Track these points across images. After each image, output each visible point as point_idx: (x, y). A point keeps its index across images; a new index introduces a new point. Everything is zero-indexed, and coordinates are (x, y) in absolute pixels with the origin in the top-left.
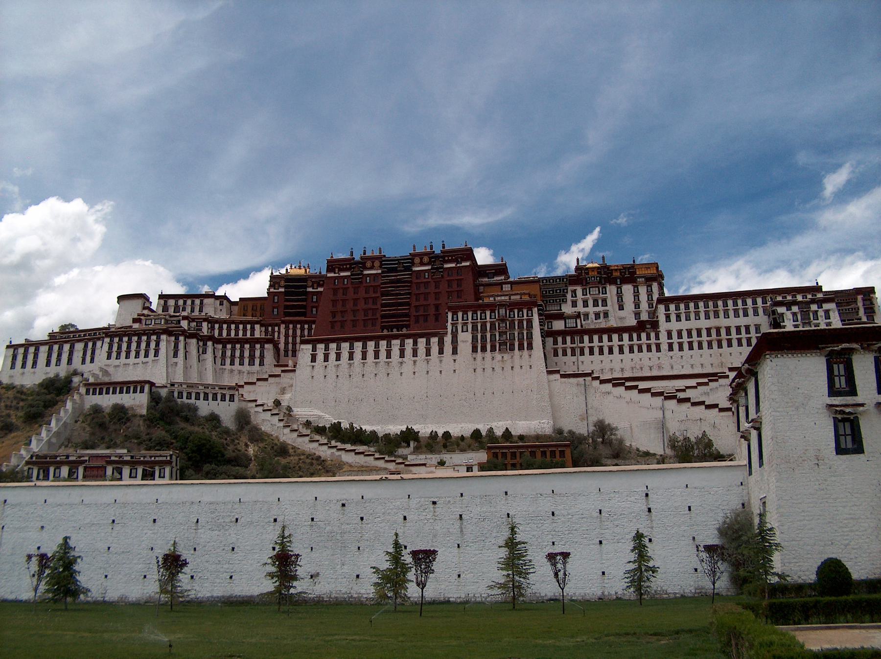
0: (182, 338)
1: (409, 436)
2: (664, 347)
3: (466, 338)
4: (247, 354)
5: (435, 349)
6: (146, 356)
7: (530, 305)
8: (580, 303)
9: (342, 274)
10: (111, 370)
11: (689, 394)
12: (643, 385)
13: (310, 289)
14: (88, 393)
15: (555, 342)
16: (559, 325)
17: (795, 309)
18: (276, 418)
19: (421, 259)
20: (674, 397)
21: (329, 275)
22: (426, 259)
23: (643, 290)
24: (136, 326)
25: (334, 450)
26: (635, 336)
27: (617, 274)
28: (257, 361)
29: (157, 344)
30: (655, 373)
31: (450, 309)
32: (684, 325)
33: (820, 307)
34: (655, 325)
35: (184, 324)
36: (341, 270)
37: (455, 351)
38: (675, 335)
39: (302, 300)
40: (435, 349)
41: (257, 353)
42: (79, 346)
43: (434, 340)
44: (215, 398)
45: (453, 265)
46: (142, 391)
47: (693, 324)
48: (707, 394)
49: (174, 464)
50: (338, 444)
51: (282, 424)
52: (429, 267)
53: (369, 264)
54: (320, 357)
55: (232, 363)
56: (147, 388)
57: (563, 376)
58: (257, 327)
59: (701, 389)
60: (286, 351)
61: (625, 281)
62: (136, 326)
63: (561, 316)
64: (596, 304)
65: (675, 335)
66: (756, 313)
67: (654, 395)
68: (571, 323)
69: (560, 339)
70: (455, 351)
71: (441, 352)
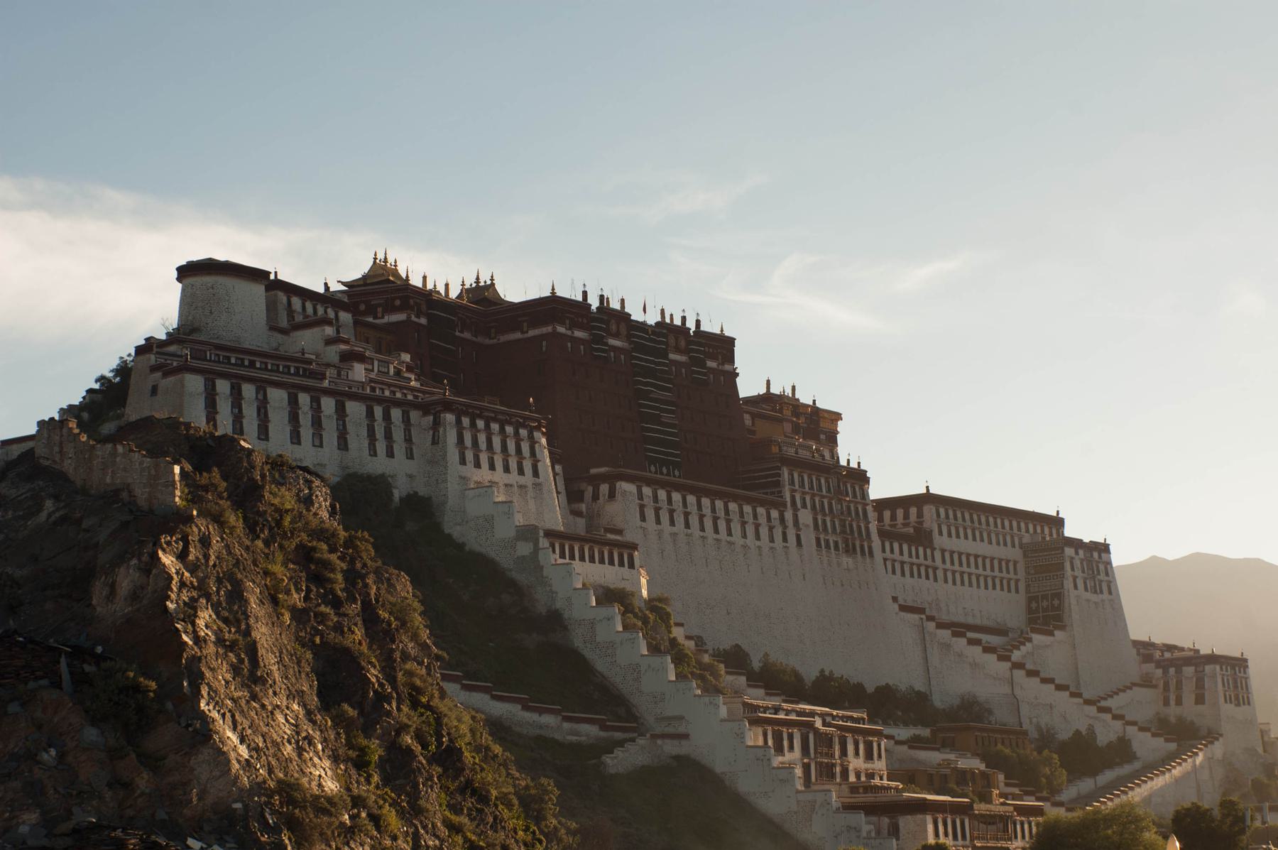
3: (806, 517)
6: (521, 471)
9: (579, 334)
12: (985, 638)
13: (457, 334)
19: (676, 339)
20: (1018, 666)
21: (561, 329)
22: (683, 343)
36: (574, 325)
42: (355, 409)
43: (775, 514)
54: (650, 513)
57: (904, 608)
67: (1002, 658)
71: (785, 539)
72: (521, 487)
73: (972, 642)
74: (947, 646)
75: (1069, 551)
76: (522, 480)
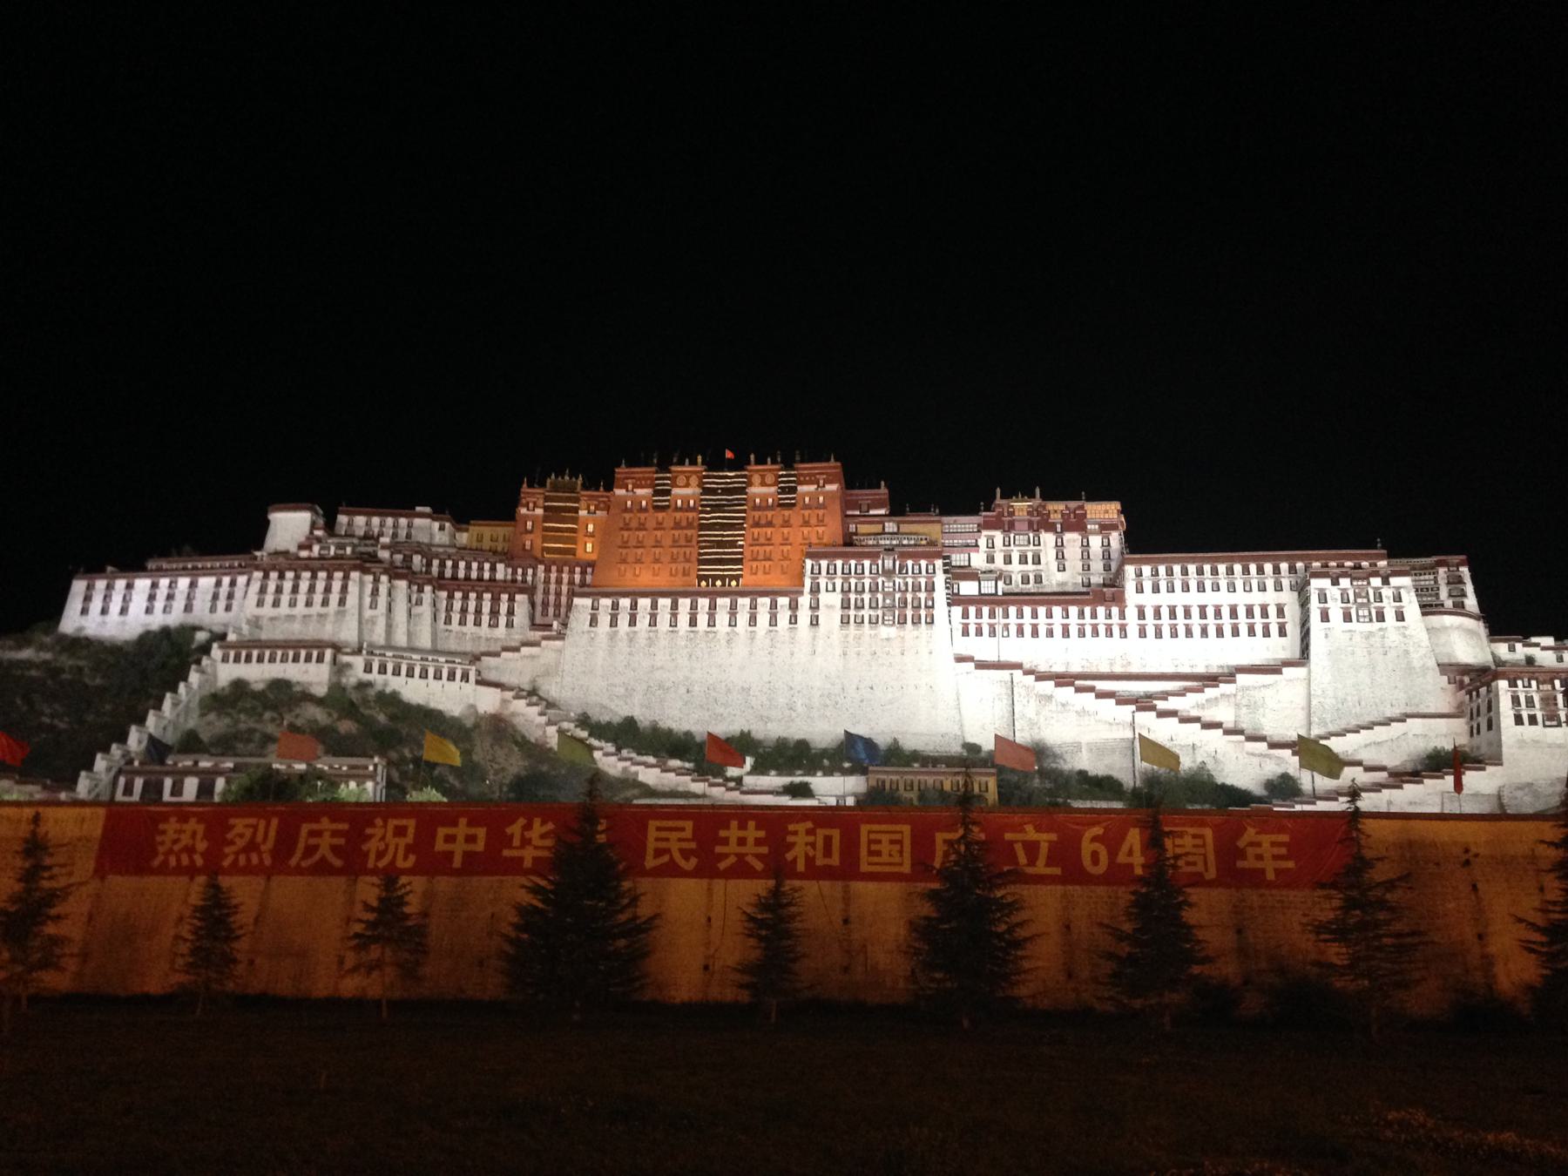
0: (384, 578)
1: (739, 746)
2: (1133, 630)
3: (831, 600)
4: (486, 608)
5: (784, 616)
6: (325, 603)
7: (930, 556)
8: (999, 558)
10: (264, 622)
11: (1173, 703)
12: (1102, 685)
14: (225, 659)
15: (965, 615)
16: (968, 588)
17: (1345, 582)
18: (536, 709)
19: (763, 477)
20: (1153, 708)
21: (620, 492)
22: (770, 478)
23: (1096, 542)
24: (304, 554)
25: (628, 763)
26: (1087, 610)
27: (1056, 518)
28: (503, 620)
29: (344, 589)
30: (1118, 669)
31: (811, 556)
32: (1164, 599)
33: (1386, 582)
34: (1119, 599)
35: (384, 555)
37: (815, 622)
38: (1149, 613)
39: (568, 530)
40: (784, 616)
41: (504, 608)
43: (783, 601)
44: (438, 677)
45: (813, 488)
46: (320, 659)
47: (1179, 599)
48: (1202, 707)
49: (379, 779)
50: (634, 755)
51: (544, 719)
52: (773, 489)
53: (681, 480)
54: (604, 619)
55: (462, 622)
56: (328, 653)
58: (500, 567)
59: (1192, 698)
60: (545, 604)
61: (1068, 527)
62: (304, 554)
63: (970, 574)
64: (1023, 560)
65: (1149, 613)
66: (1278, 587)
67: (1122, 701)
68: (988, 587)
69: (972, 610)
70: (815, 622)
71: (793, 620)
72: (320, 615)
73: (1079, 690)
74: (1050, 698)
75: (1316, 584)
76: (324, 610)
